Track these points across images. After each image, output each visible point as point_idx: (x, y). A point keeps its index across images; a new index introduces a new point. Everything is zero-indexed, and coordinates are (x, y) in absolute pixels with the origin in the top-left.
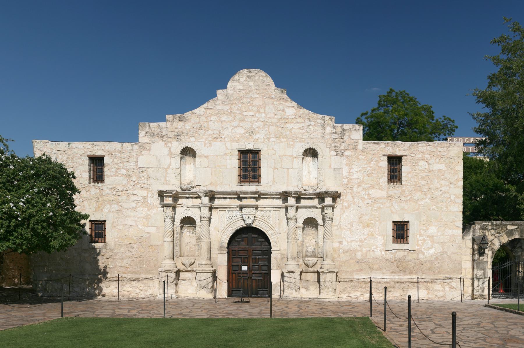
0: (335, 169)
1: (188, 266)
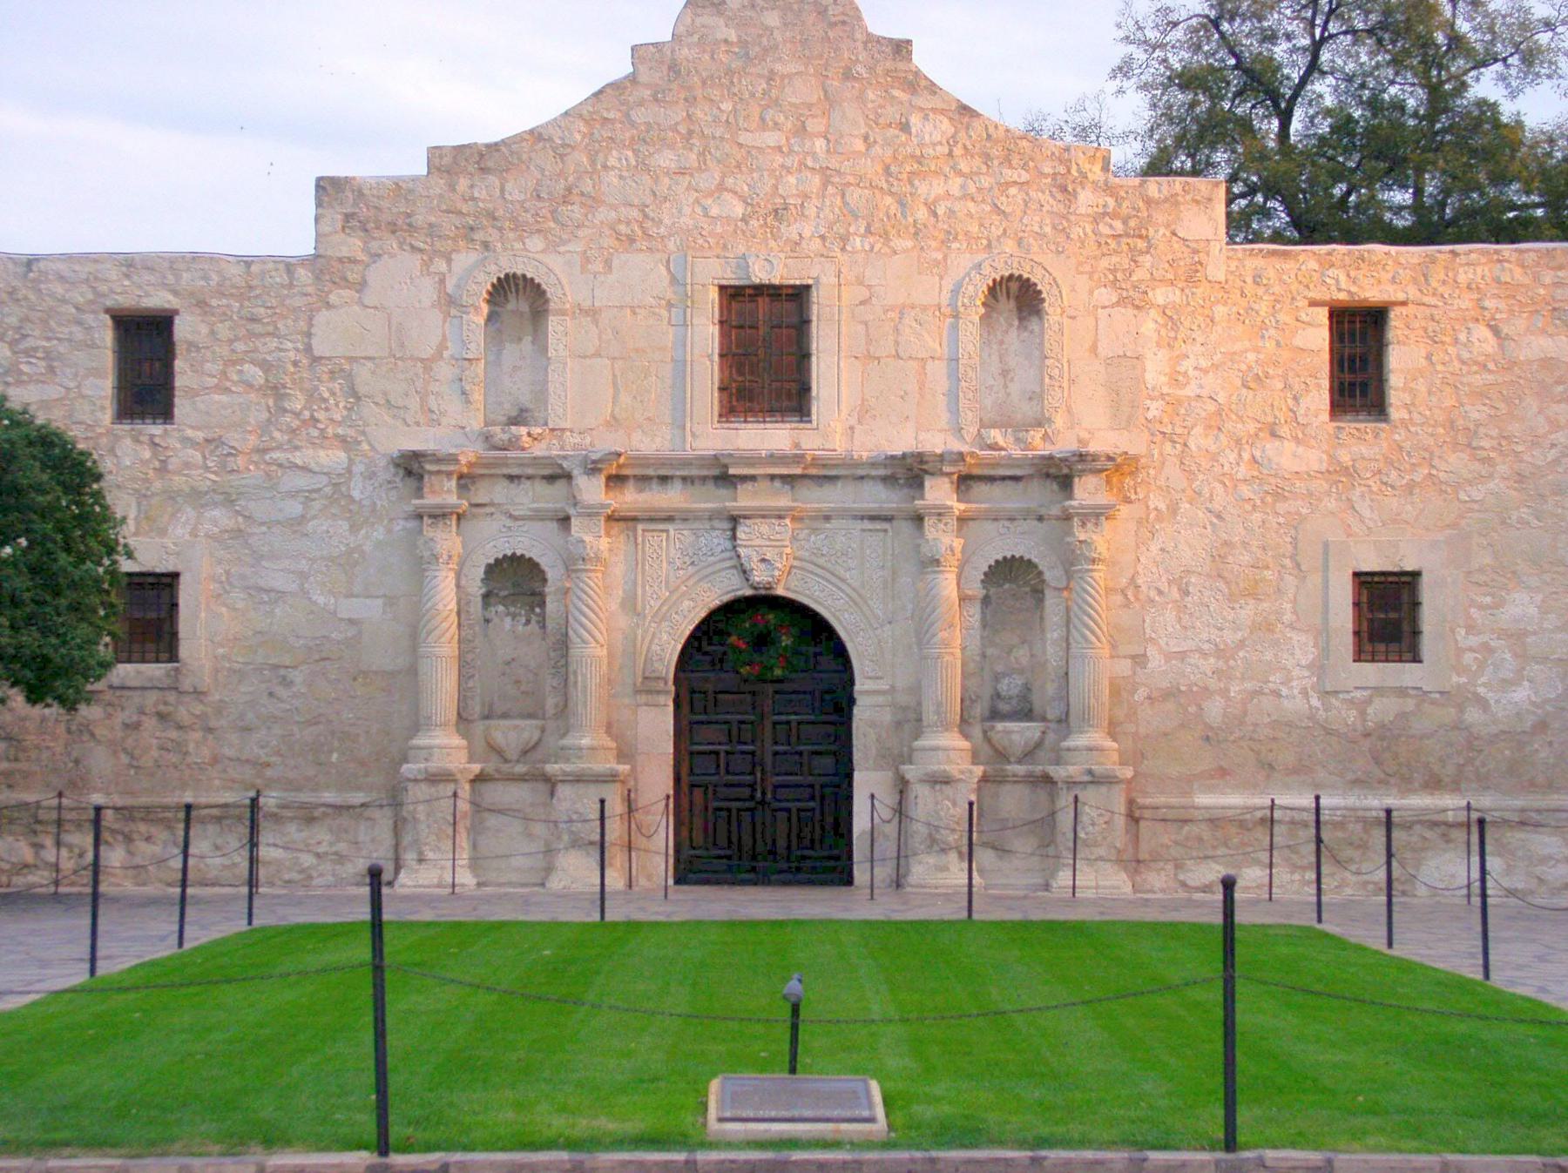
0: (1109, 361)
1: (515, 757)
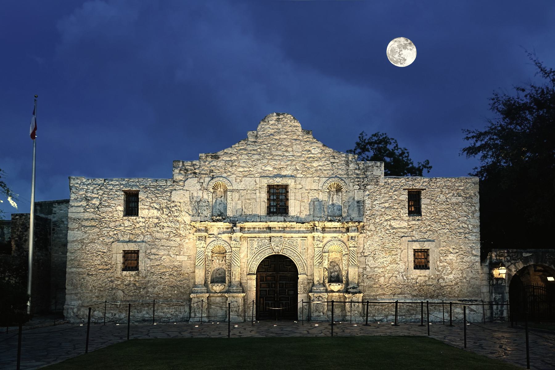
0: (358, 202)
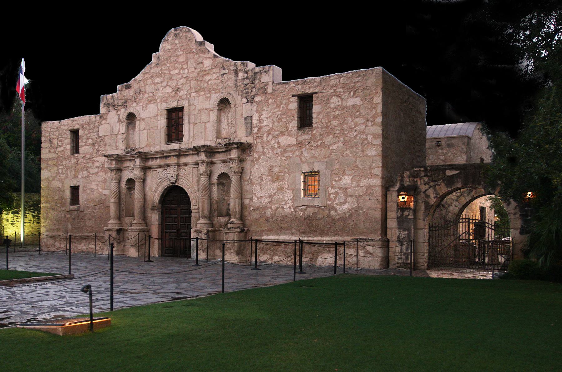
0: (246, 119)
